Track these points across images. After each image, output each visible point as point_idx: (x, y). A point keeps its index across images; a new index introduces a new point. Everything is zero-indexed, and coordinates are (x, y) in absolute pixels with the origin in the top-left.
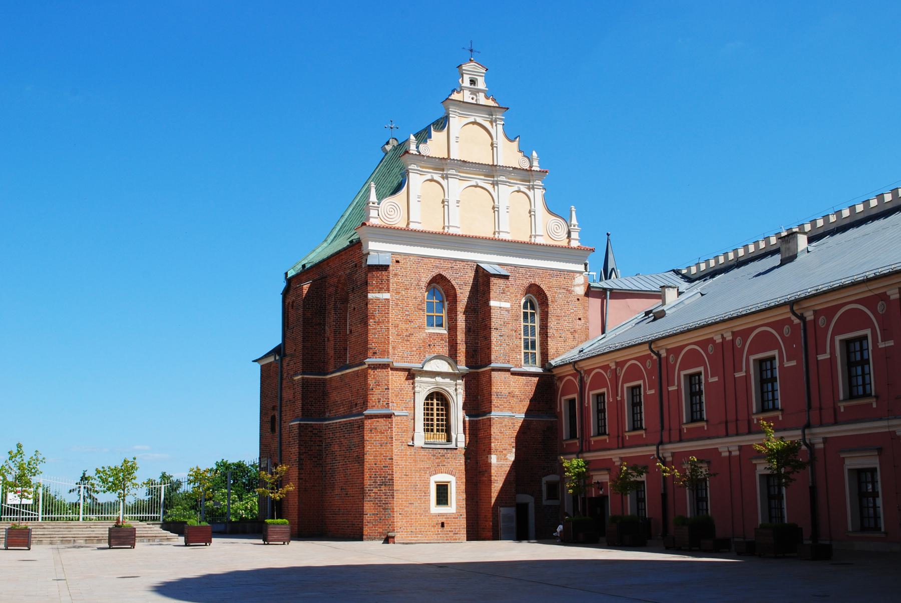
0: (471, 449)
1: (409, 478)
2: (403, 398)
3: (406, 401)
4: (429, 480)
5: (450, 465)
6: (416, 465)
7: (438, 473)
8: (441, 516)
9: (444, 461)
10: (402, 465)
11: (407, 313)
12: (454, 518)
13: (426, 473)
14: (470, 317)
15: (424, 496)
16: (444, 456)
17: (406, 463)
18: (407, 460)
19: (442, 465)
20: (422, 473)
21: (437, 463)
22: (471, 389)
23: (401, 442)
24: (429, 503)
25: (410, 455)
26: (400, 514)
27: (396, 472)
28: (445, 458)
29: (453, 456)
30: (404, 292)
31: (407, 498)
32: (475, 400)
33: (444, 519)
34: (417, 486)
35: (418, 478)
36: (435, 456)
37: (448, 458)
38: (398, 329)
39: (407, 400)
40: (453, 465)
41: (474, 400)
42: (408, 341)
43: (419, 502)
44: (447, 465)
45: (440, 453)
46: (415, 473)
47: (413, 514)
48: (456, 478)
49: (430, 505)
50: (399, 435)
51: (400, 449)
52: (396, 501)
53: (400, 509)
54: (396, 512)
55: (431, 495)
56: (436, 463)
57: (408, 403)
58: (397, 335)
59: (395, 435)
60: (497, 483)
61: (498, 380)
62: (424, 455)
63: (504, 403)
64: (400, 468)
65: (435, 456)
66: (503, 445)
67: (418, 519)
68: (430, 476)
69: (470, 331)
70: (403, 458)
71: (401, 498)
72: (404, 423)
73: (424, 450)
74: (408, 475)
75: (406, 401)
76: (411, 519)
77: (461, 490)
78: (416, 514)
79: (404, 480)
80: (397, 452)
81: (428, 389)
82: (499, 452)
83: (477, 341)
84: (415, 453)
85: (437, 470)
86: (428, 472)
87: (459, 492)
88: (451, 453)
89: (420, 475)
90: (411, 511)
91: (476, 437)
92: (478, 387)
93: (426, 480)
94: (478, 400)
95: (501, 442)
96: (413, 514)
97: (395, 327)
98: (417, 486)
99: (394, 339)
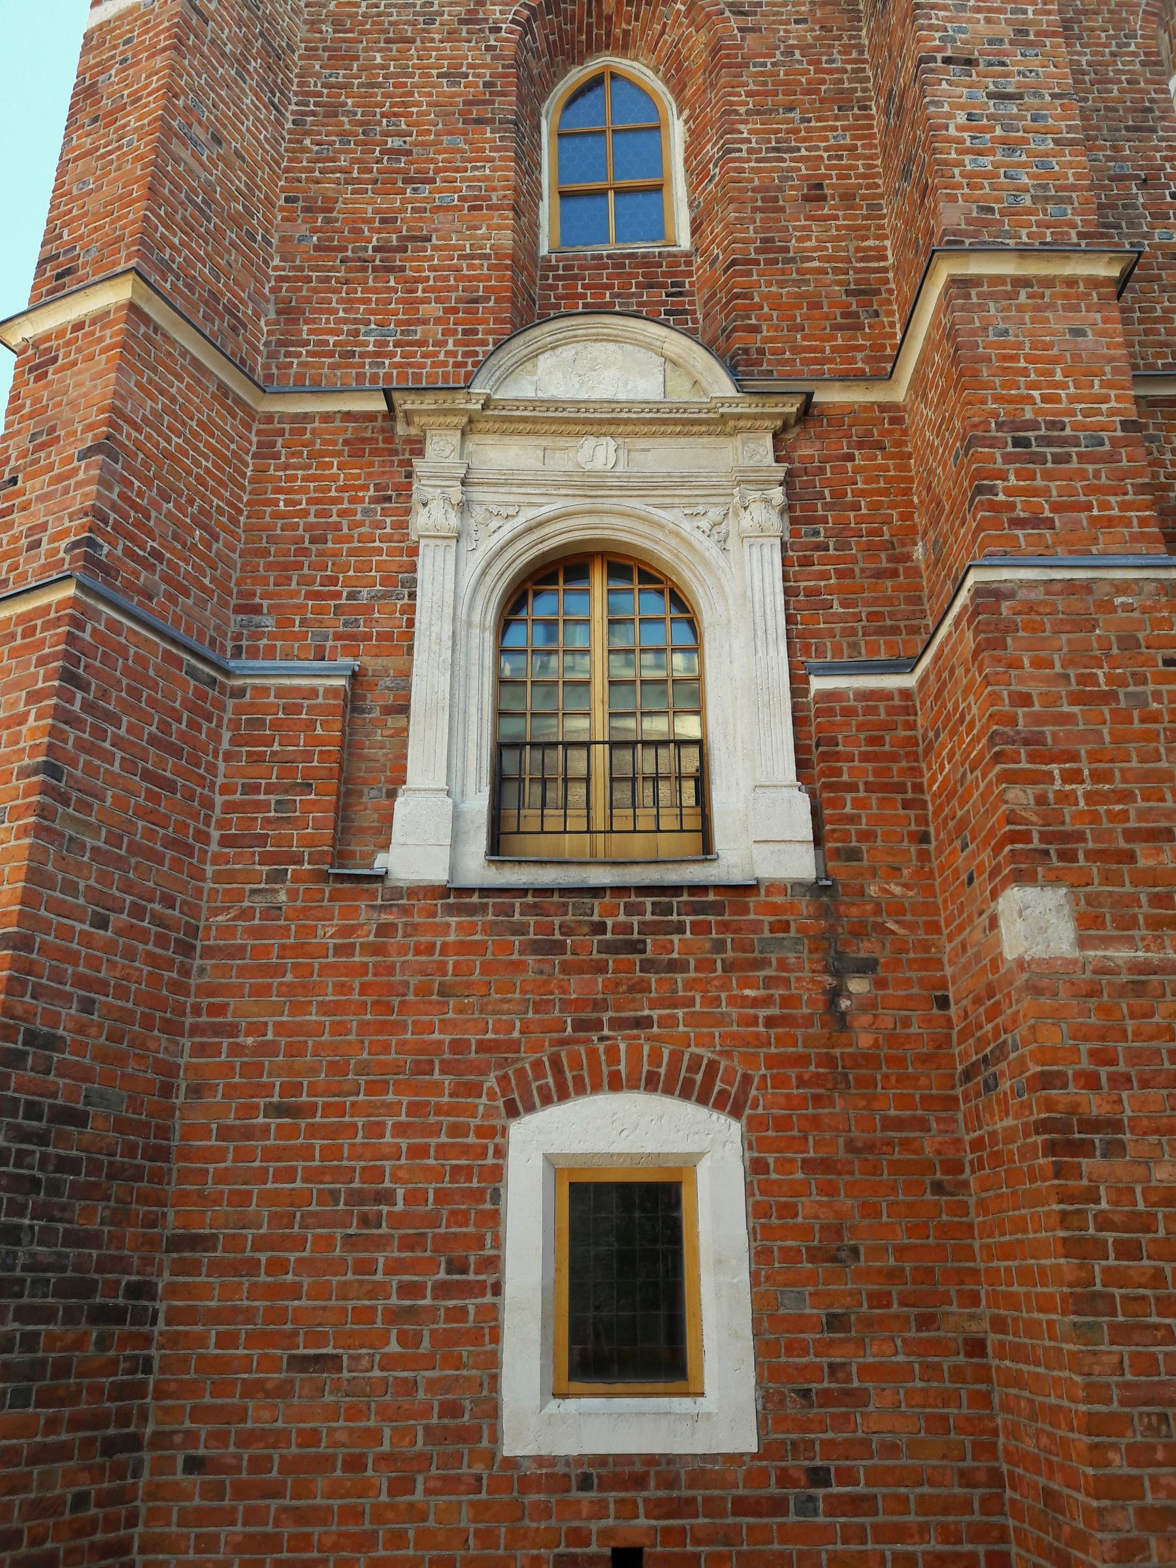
0: (873, 890)
1: (314, 1131)
2: (333, 581)
3: (352, 596)
4: (501, 1152)
5: (691, 1020)
6: (383, 1027)
7: (580, 1090)
8: (605, 1484)
9: (642, 987)
10: (261, 1029)
11: (393, 143)
12: (741, 1506)
13: (474, 1090)
14: (808, 130)
15: (443, 1290)
16: (637, 947)
17: (299, 1008)
18: (307, 989)
19: (615, 1024)
20: (437, 1089)
21: (579, 1005)
22: (856, 507)
23: (265, 859)
24: (493, 1361)
25: (339, 950)
26: (194, 1465)
27: (196, 1091)
28: (647, 966)
29: (719, 946)
30: (378, 55)
31: (278, 1316)
32: (894, 574)
33: (642, 1521)
34: (386, 1197)
35: (400, 1130)
36: (559, 947)
37: (675, 966)
38: (327, 221)
39: (365, 592)
40: (721, 1020)
41: (879, 574)
42: (391, 270)
43: (394, 1347)
44: (671, 1021)
45: (600, 928)
46: (374, 1088)
47: (324, 1463)
48: (753, 1125)
49: (495, 1379)
50: (263, 806)
51: (259, 903)
52: (173, 1340)
53: (197, 1414)
54: (161, 1440)
55: (509, 1289)
56: (566, 1004)
57: (367, 610)
58: (317, 248)
59: (229, 807)
60: (1115, 1149)
61: (1019, 345)
62: (463, 947)
63: (1089, 490)
64: (235, 1050)
65: (559, 947)
66: (1126, 796)
67: (378, 1515)
68: (513, 1111)
69: (823, 198)
70: (279, 970)
71: (215, 1316)
72: (311, 725)
73: (451, 910)
74: (311, 1109)
75: (352, 596)
76: (302, 1516)
77: (805, 1232)
78: (355, 1464)
79: (269, 1156)
80: (227, 931)
81: (520, 522)
82: (1091, 855)
83: (871, 243)
84: (385, 930)
85: (576, 1064)
86: (491, 1082)
87: (790, 1256)
88: (700, 929)
89: (414, 1109)
90: (311, 1438)
91: (907, 805)
92: (908, 492)
93: (465, 1150)
94: (916, 572)
95: (1097, 777)
96: (324, 1463)
97: (306, 210)
98: (386, 1197)
99: (301, 269)
